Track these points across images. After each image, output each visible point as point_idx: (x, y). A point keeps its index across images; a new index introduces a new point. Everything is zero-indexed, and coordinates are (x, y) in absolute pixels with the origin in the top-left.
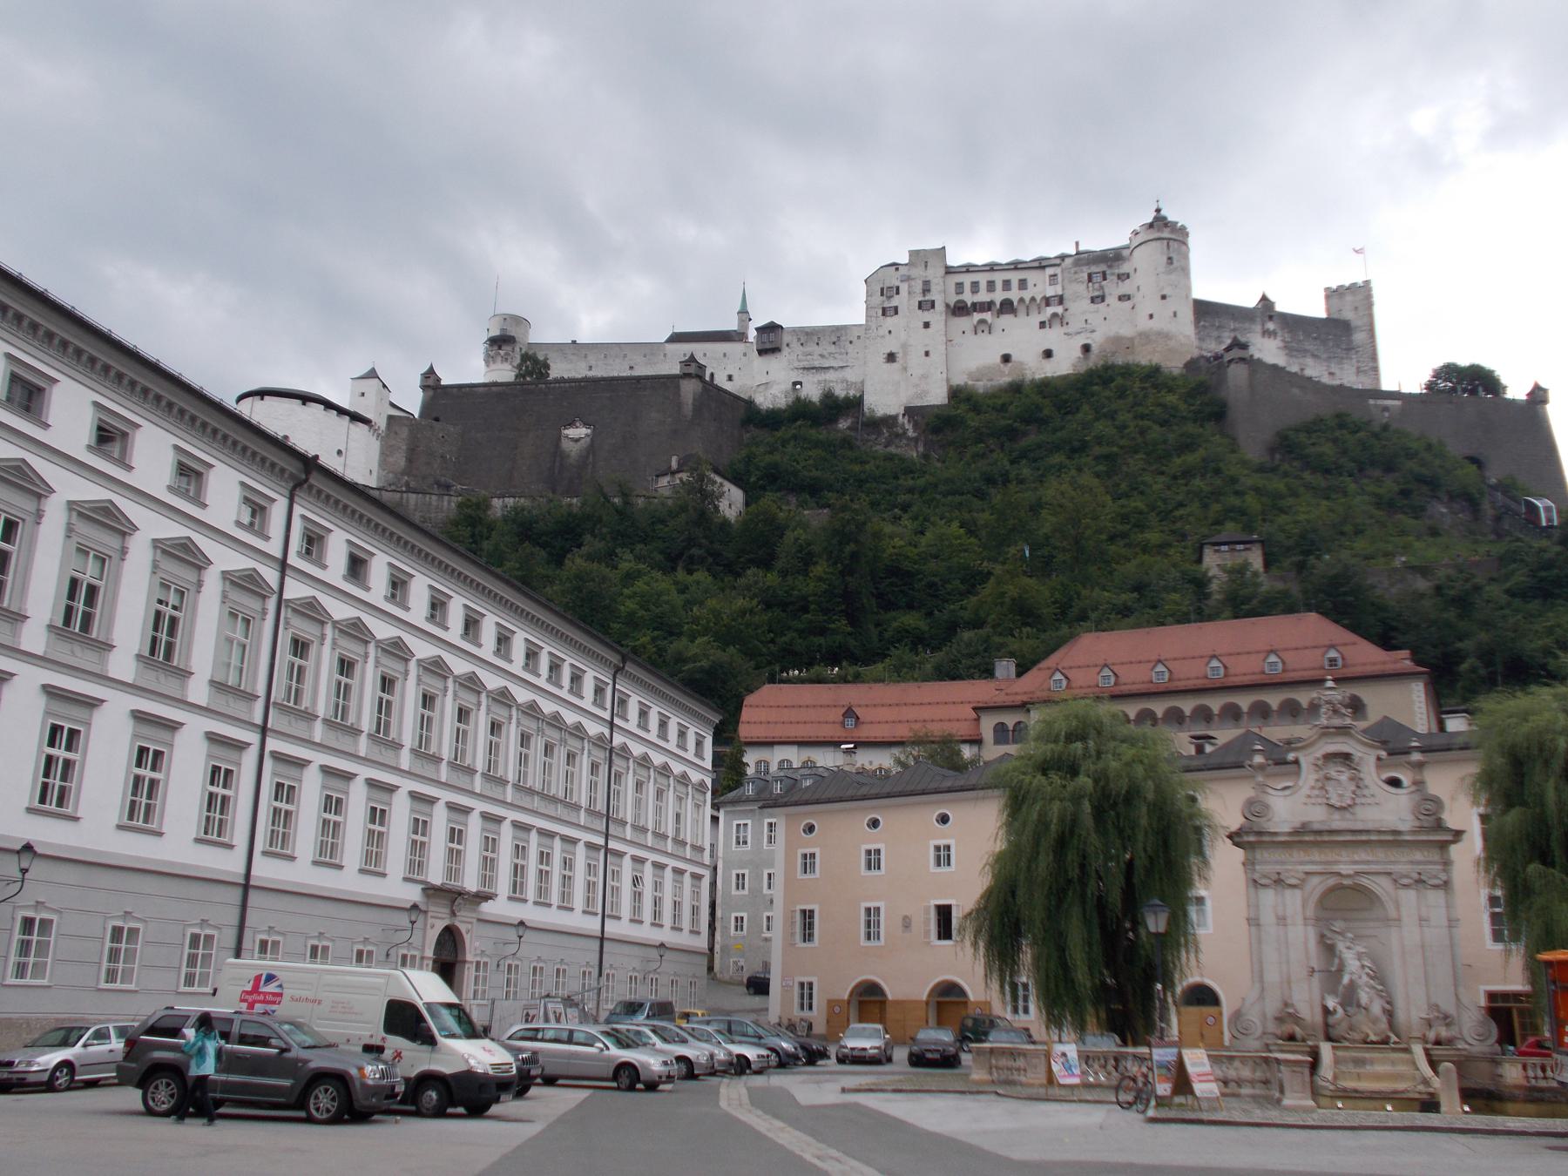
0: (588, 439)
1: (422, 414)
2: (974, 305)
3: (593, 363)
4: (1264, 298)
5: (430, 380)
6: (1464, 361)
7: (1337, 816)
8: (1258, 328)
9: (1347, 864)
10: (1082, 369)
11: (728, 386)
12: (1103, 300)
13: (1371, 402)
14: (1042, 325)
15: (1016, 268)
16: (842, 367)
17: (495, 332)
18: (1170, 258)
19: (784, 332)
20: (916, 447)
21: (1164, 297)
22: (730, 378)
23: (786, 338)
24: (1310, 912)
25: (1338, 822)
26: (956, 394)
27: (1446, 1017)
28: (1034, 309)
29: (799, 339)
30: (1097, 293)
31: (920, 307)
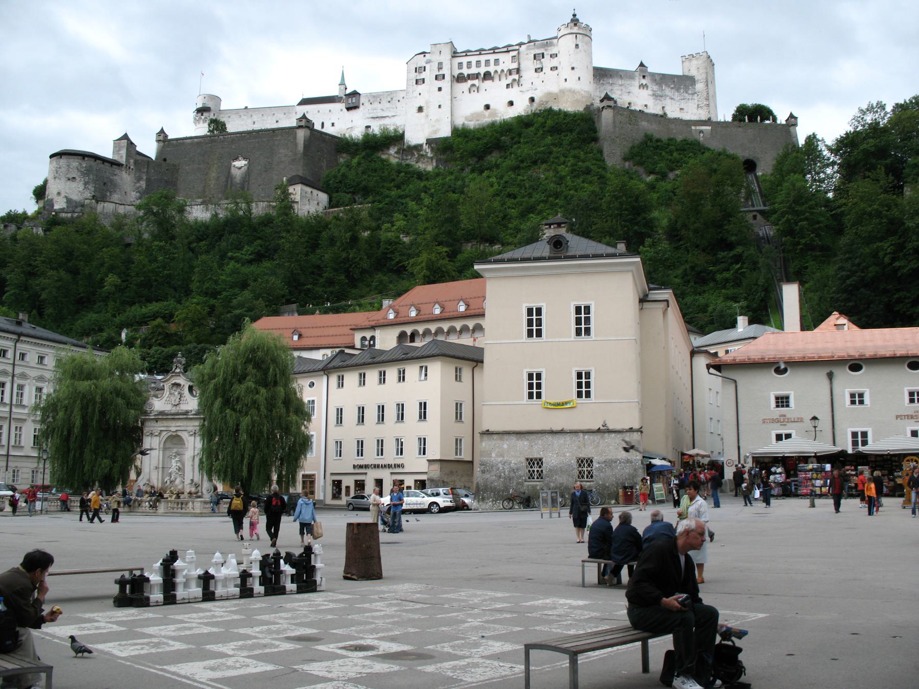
0: (246, 167)
1: (156, 159)
2: (469, 75)
3: (255, 120)
4: (642, 65)
6: (750, 102)
7: (174, 408)
9: (174, 426)
12: (542, 70)
13: (693, 128)
14: (508, 86)
15: (494, 53)
17: (200, 106)
18: (577, 46)
19: (361, 96)
21: (573, 68)
23: (362, 100)
24: (162, 446)
25: (174, 410)
26: (456, 131)
27: (196, 484)
28: (503, 78)
31: (436, 79)
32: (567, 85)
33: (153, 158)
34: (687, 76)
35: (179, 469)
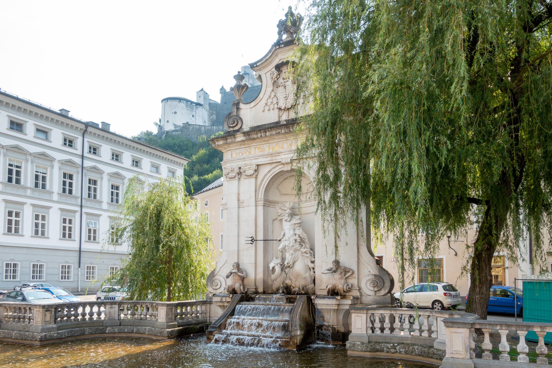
5: (222, 90)
24: (261, 196)
33: (219, 102)
35: (302, 242)
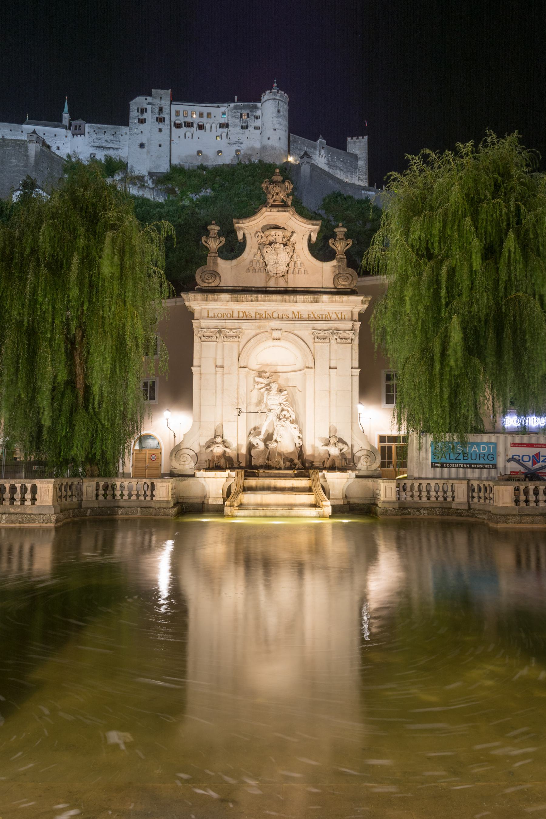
8: (318, 153)
10: (235, 163)
11: (58, 152)
12: (247, 128)
13: (363, 192)
16: (117, 148)
20: (153, 193)
22: (58, 148)
26: (173, 168)
29: (94, 131)
30: (244, 124)
32: (270, 143)
34: (352, 154)
